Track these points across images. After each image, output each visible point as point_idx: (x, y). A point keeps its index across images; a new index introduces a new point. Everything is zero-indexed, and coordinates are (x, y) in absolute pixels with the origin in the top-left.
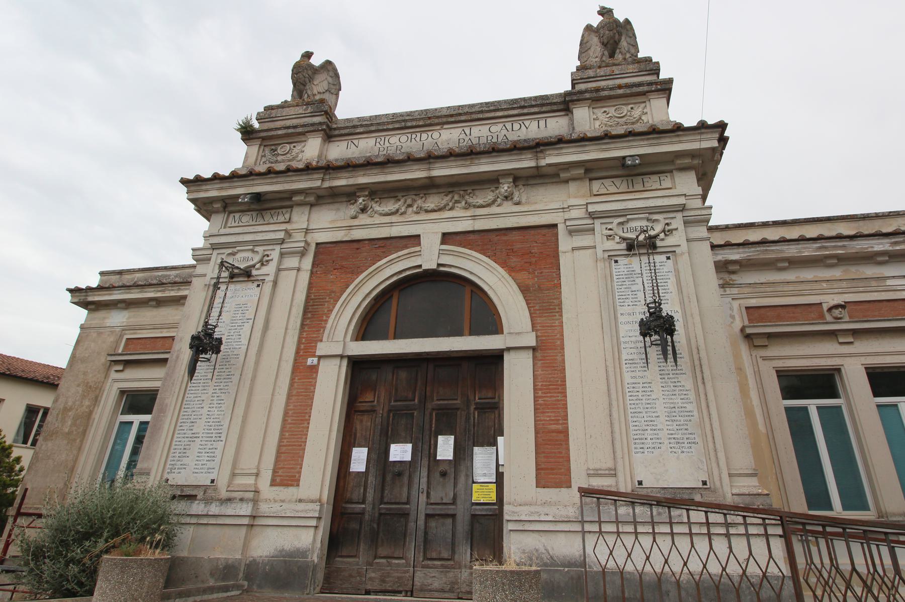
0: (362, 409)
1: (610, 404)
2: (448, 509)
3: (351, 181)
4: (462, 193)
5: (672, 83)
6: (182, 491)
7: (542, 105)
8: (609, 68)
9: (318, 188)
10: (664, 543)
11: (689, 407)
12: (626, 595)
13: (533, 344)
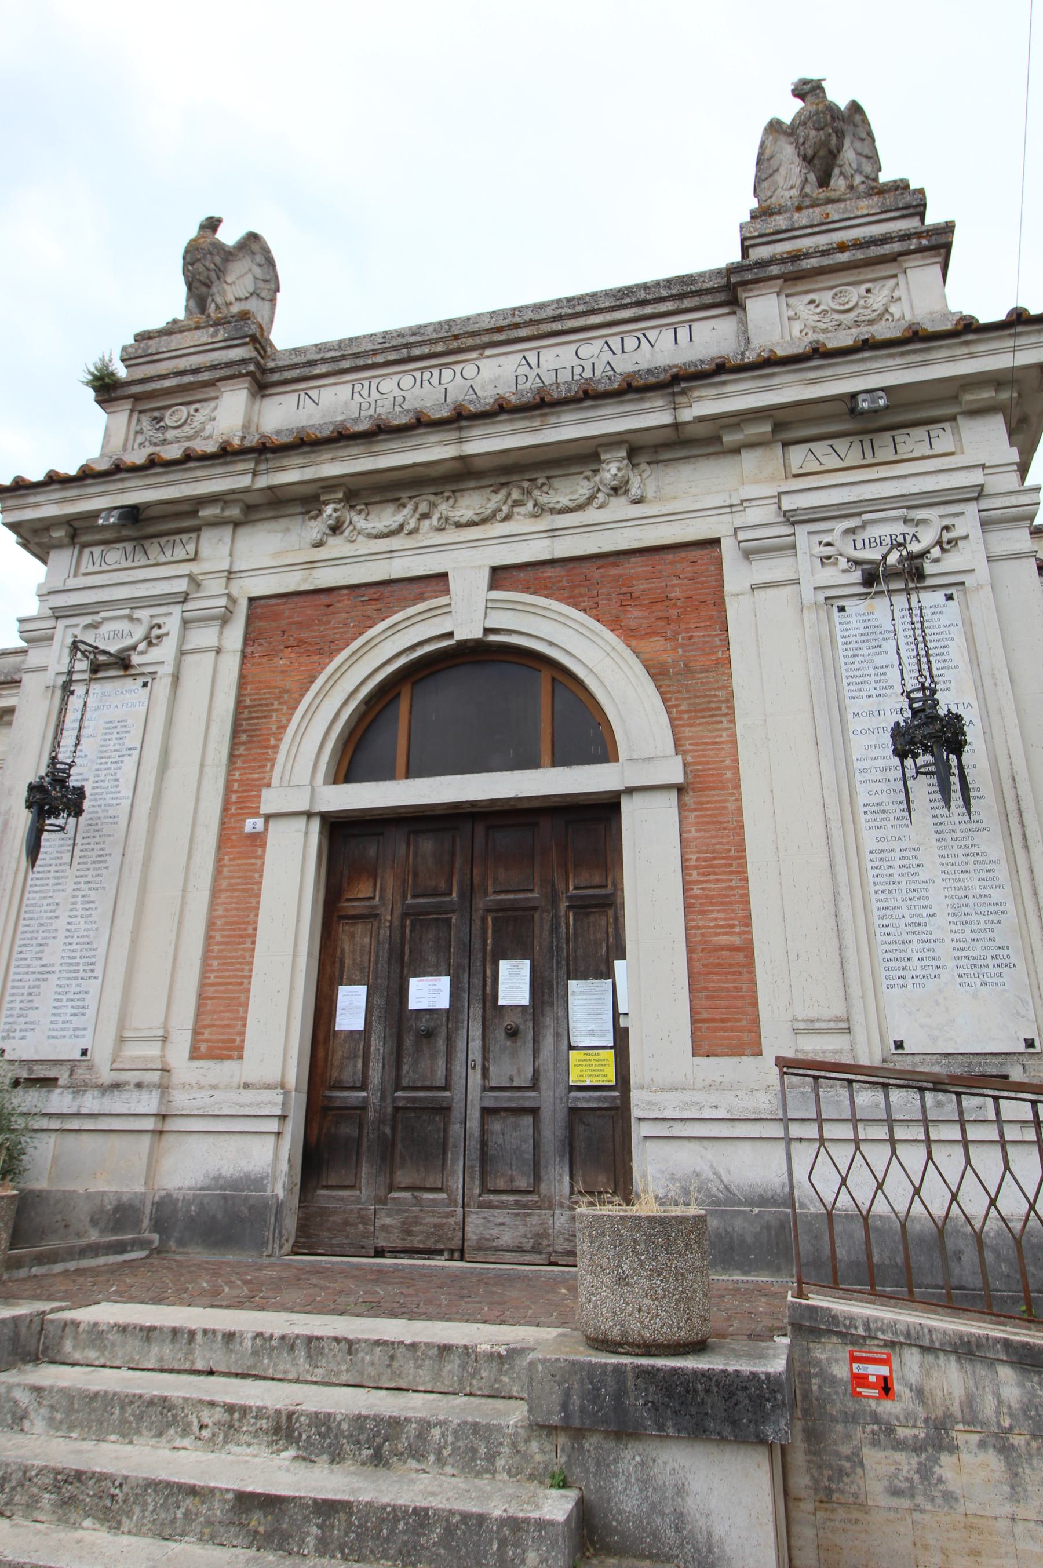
0: (351, 912)
1: (836, 894)
2: (523, 1098)
3: (309, 474)
4: (526, 484)
5: (952, 232)
6: (30, 1070)
7: (682, 296)
8: (818, 210)
9: (247, 490)
10: (950, 1160)
11: (996, 895)
12: (876, 1259)
13: (678, 778)
